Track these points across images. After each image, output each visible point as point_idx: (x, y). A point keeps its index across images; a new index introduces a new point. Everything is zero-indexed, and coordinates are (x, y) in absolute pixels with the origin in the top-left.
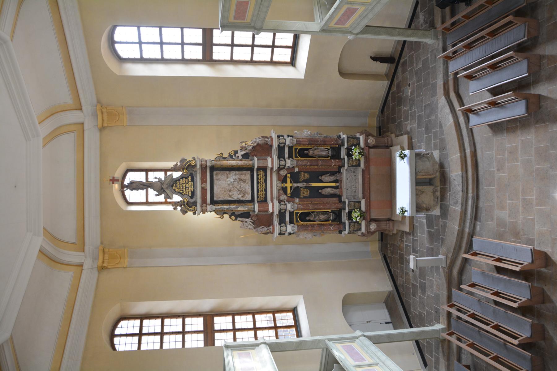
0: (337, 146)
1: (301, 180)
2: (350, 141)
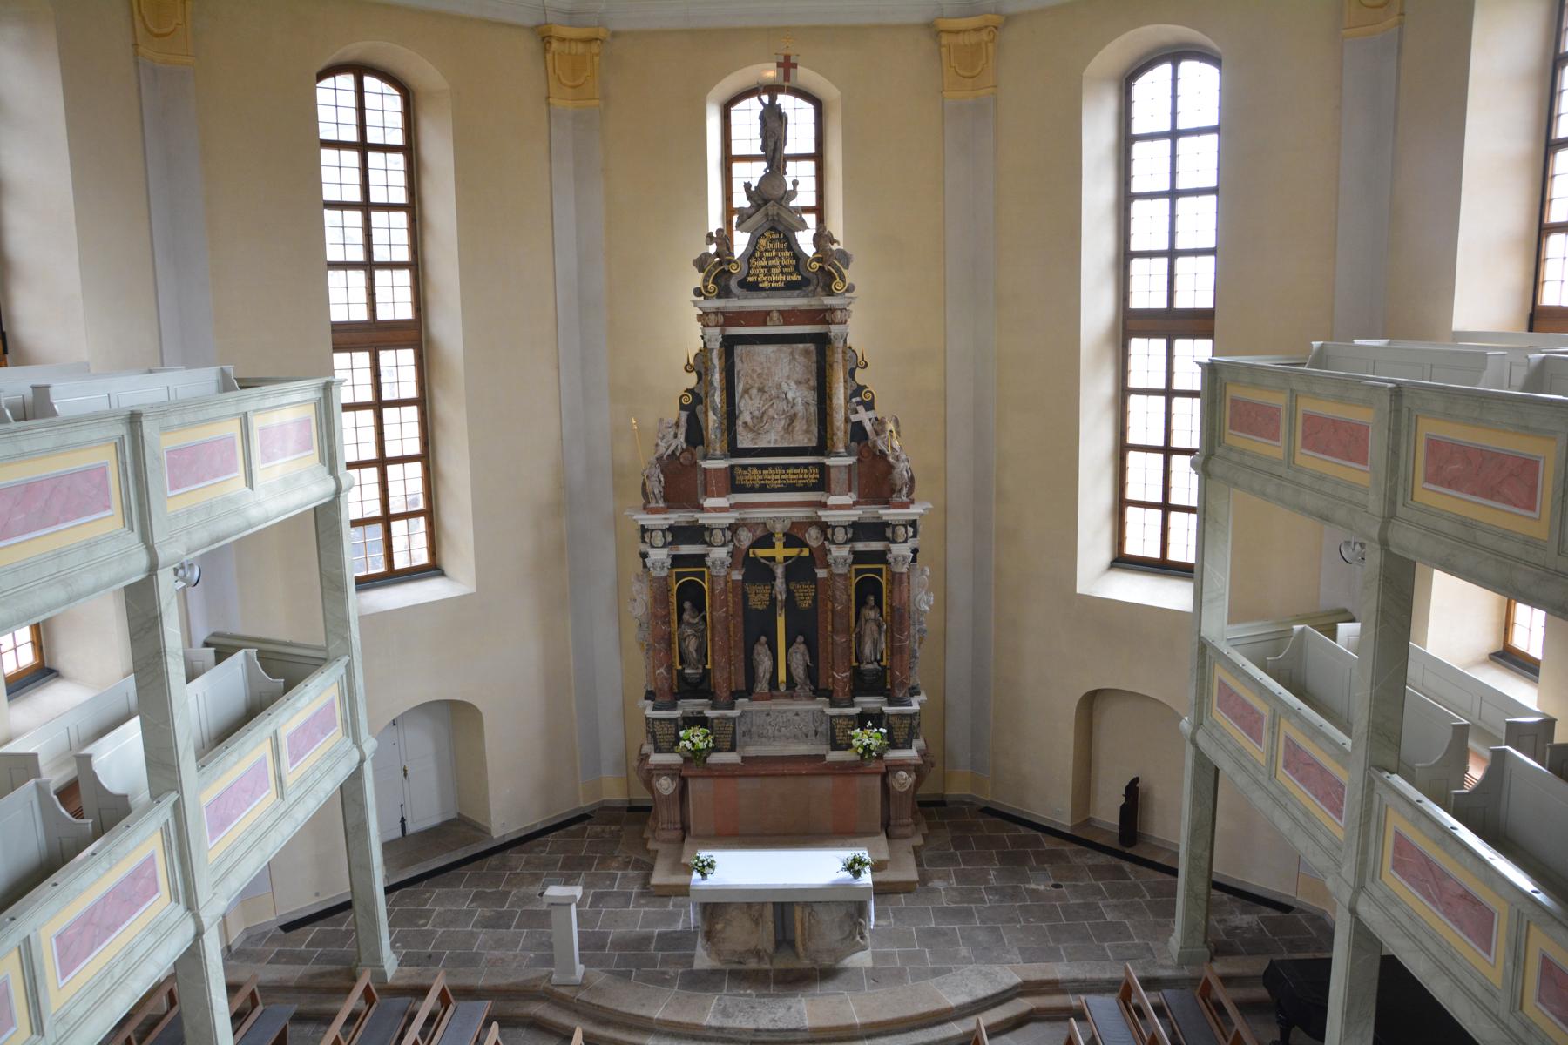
0: (889, 687)
2: (902, 723)
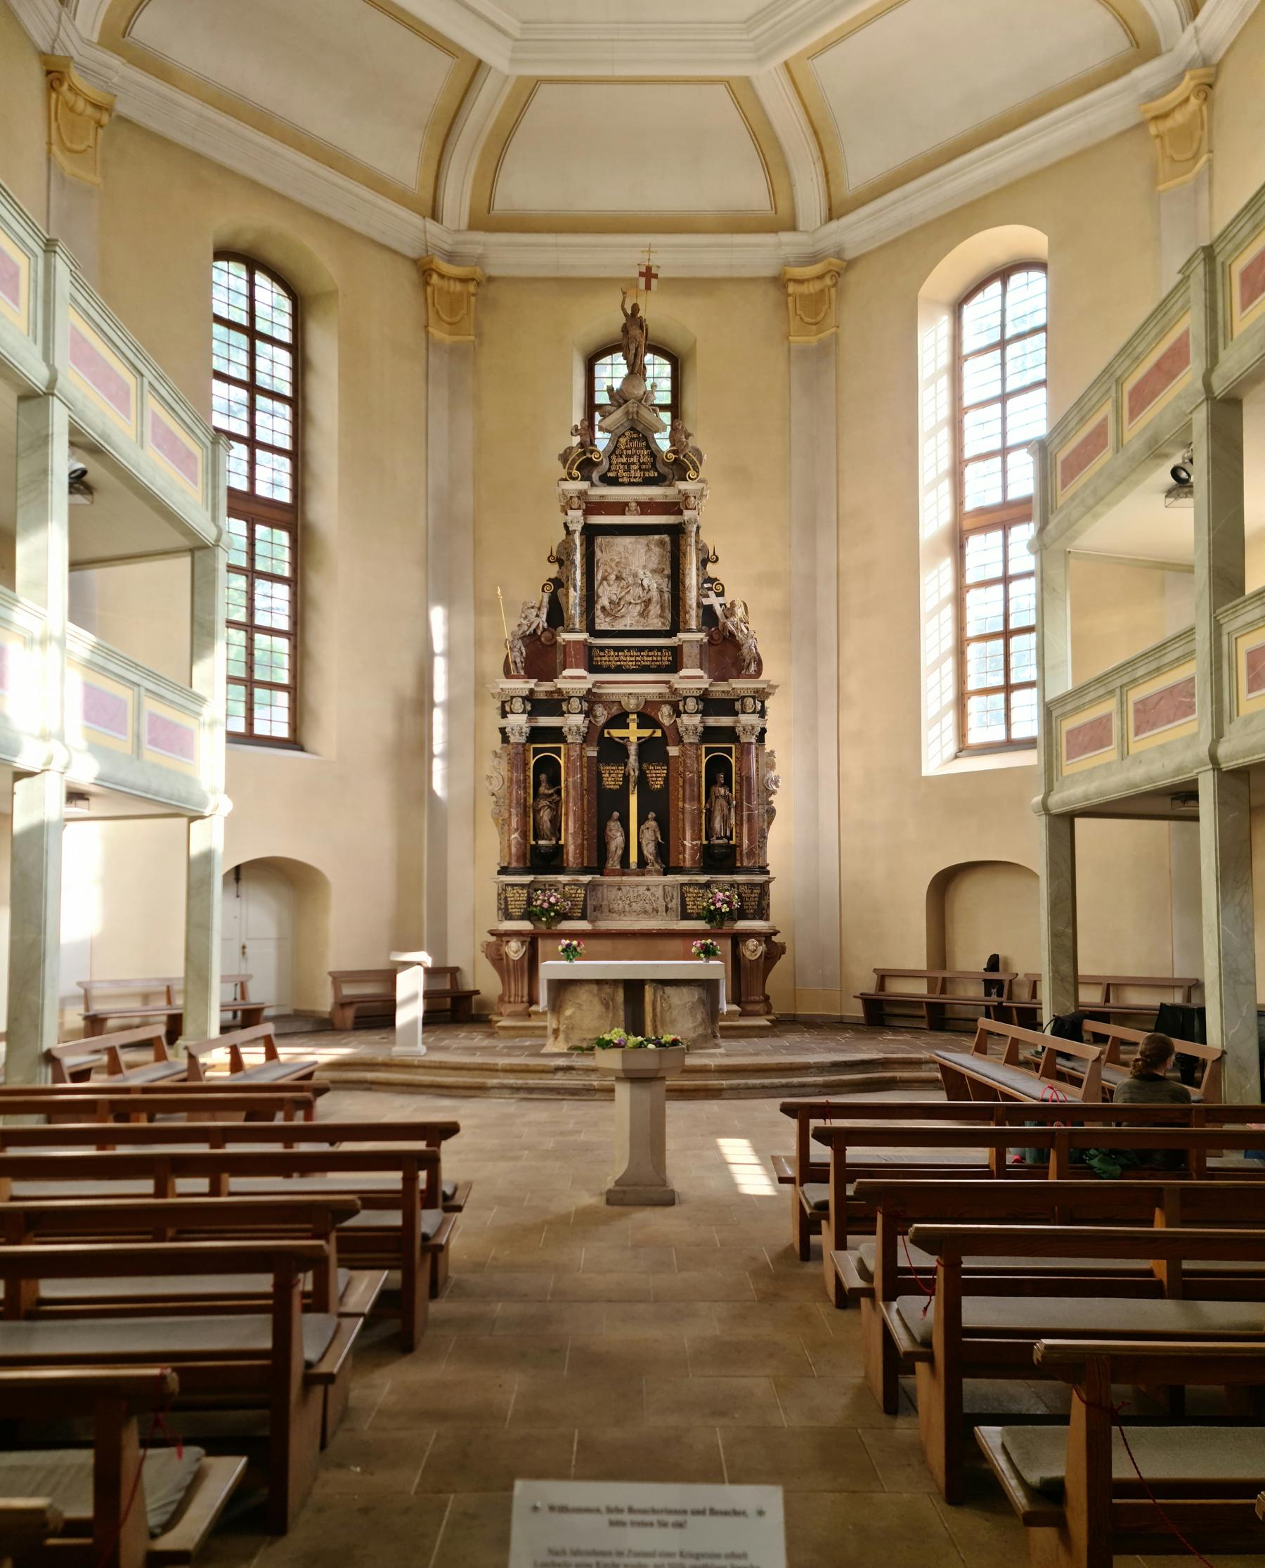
0: (738, 864)
2: (752, 893)
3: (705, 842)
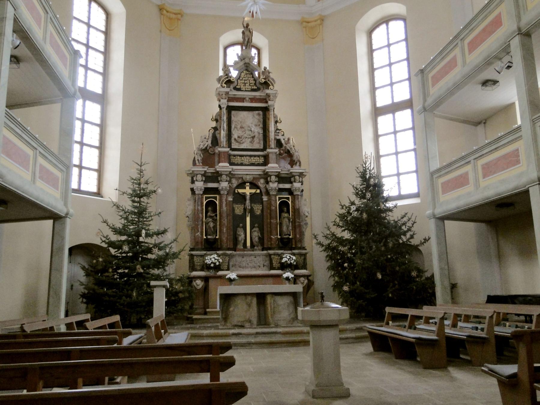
1: (253, 205)
2: (301, 258)
3: (279, 237)
